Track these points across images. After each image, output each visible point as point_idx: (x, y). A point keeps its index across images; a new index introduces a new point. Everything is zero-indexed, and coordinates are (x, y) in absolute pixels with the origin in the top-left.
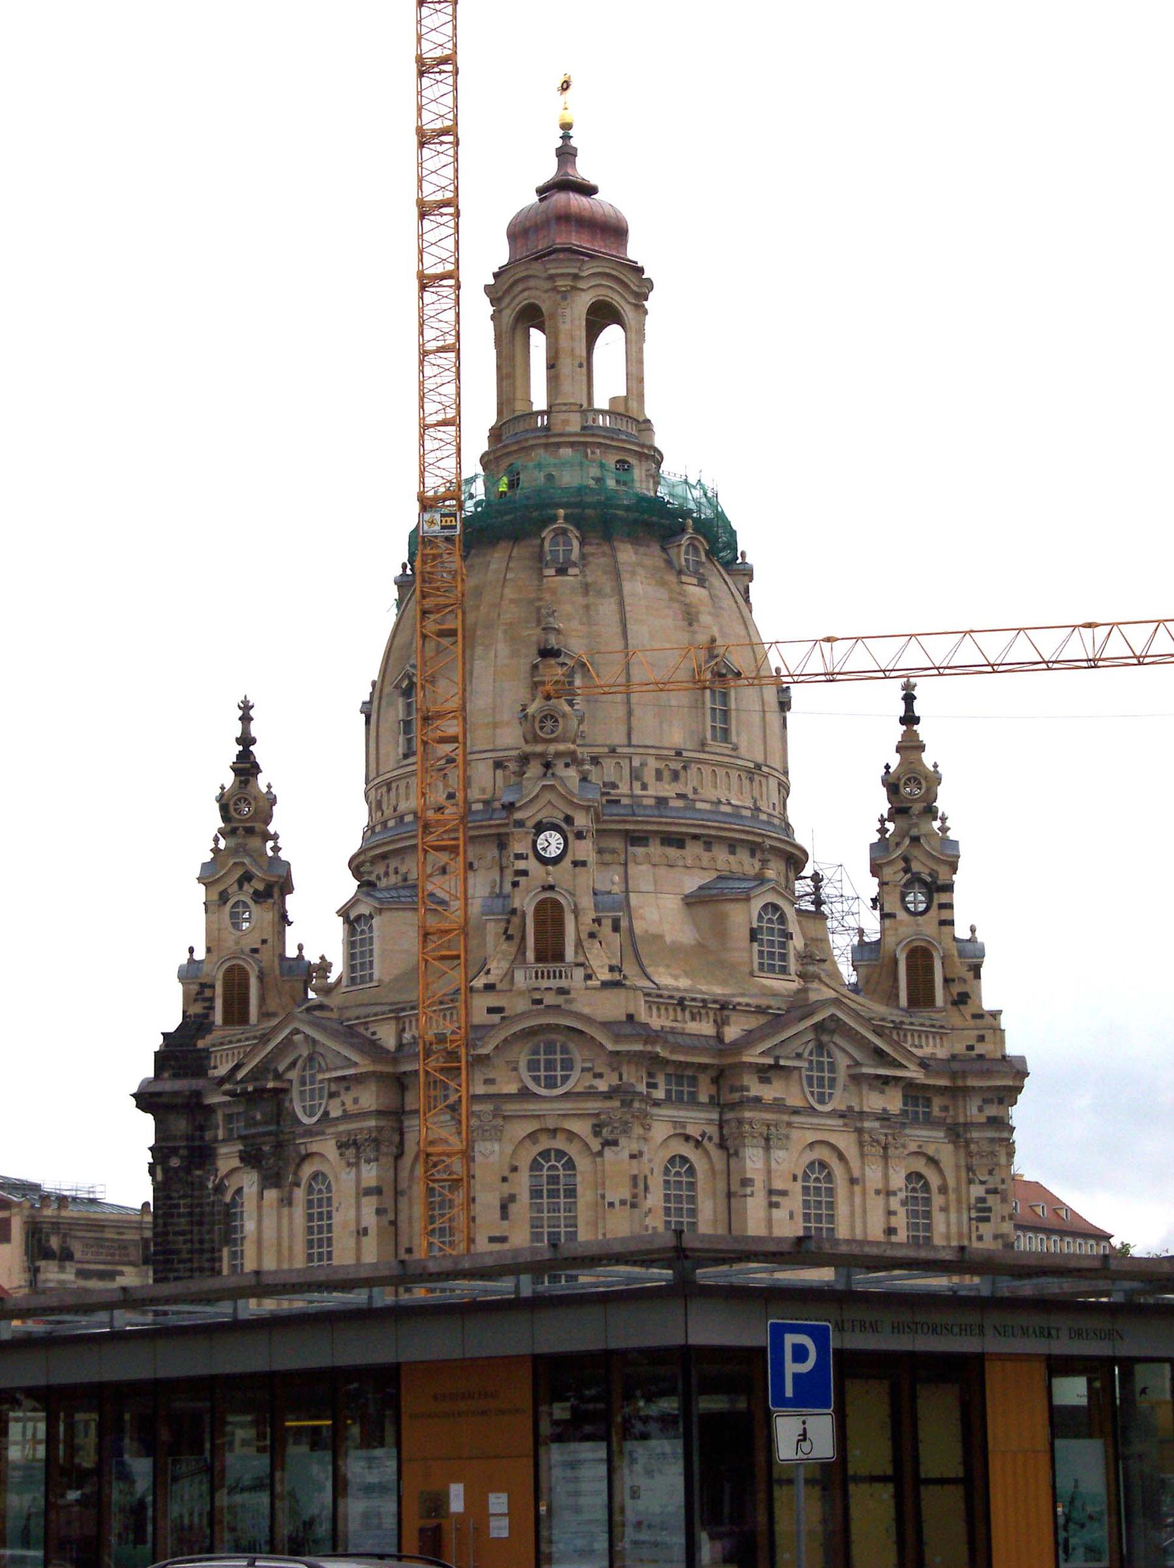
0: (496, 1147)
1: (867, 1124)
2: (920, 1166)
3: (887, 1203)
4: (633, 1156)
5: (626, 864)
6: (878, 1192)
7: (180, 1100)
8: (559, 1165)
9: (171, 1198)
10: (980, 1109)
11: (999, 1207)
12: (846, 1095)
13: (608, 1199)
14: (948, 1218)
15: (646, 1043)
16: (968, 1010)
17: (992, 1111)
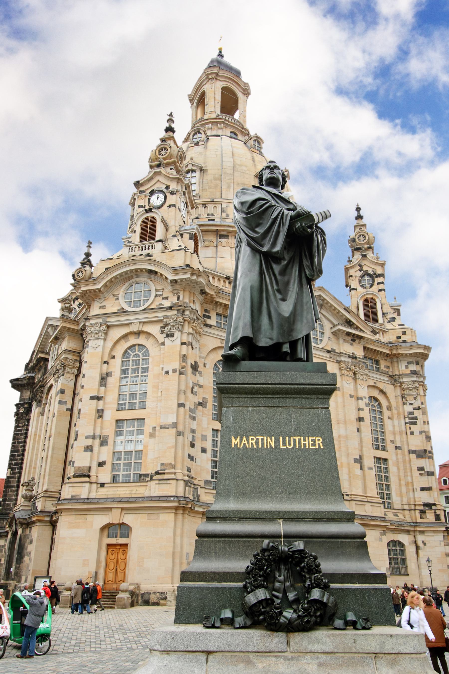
0: (101, 342)
1: (343, 359)
2: (376, 393)
3: (358, 404)
4: (183, 344)
5: (217, 246)
6: (351, 396)
7: (25, 382)
8: (140, 354)
9: (20, 427)
10: (407, 367)
11: (421, 416)
12: (330, 342)
13: (165, 369)
14: (393, 423)
15: (192, 274)
16: (396, 323)
17: (413, 367)
